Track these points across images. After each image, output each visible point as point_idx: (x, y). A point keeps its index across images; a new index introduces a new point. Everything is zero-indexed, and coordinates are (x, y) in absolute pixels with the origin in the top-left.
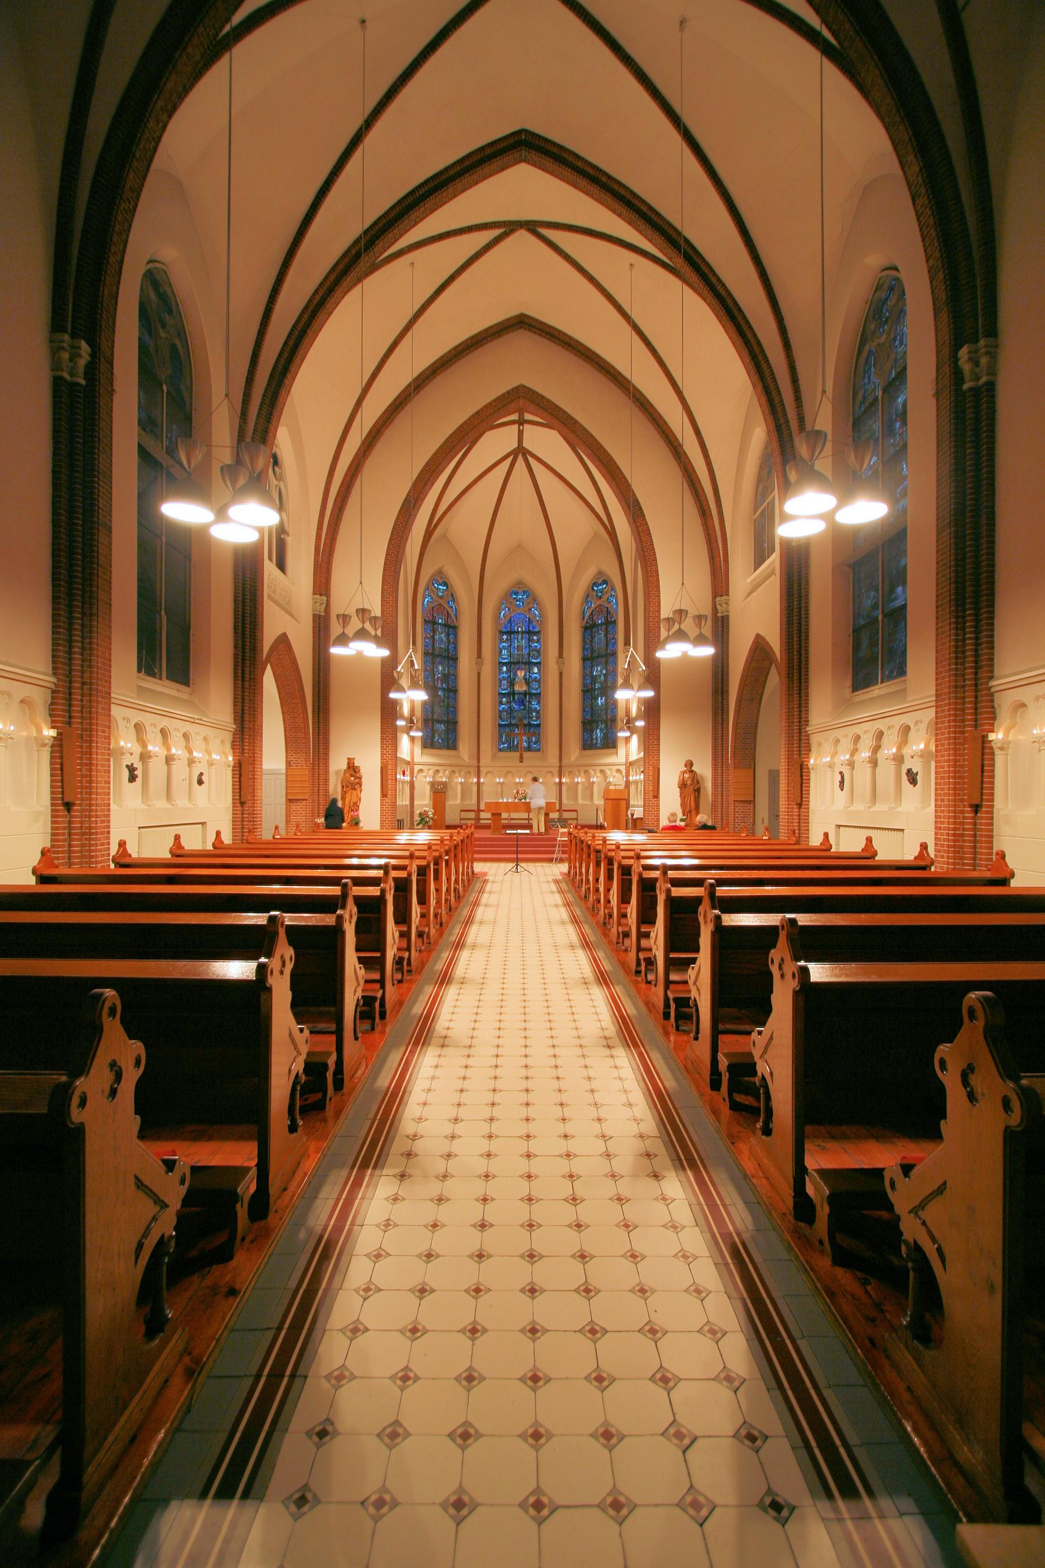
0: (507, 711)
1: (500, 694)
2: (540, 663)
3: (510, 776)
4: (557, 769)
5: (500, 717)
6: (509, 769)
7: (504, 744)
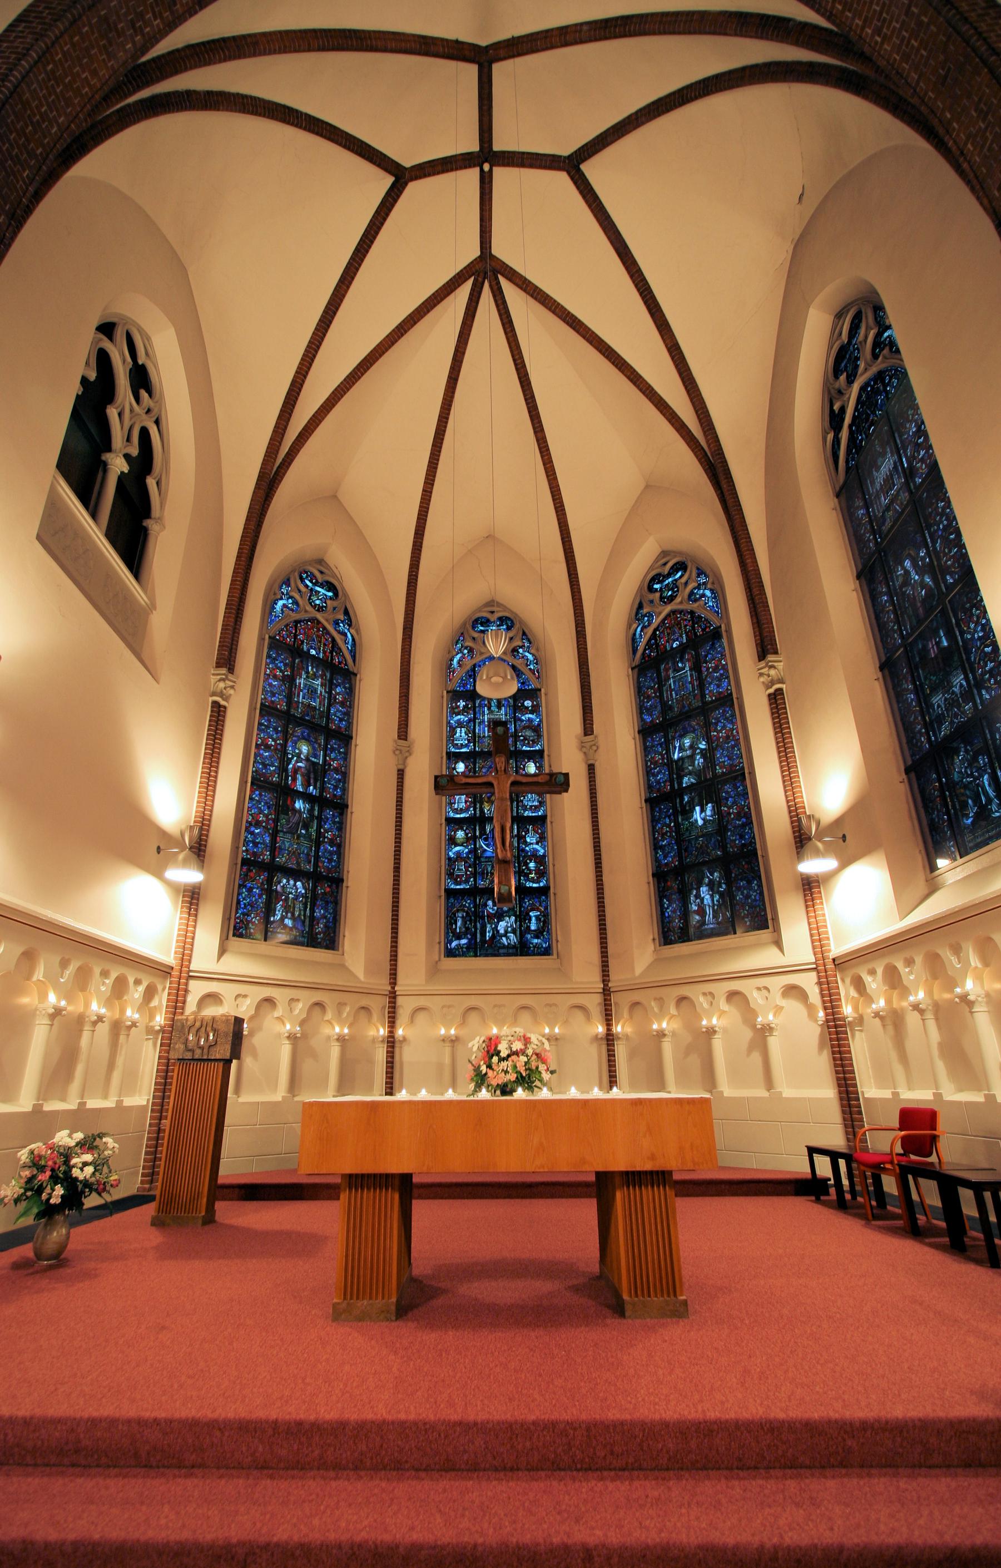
0: (465, 860)
1: (449, 821)
2: (541, 753)
3: (473, 1018)
4: (598, 999)
5: (450, 875)
6: (473, 1001)
7: (459, 937)
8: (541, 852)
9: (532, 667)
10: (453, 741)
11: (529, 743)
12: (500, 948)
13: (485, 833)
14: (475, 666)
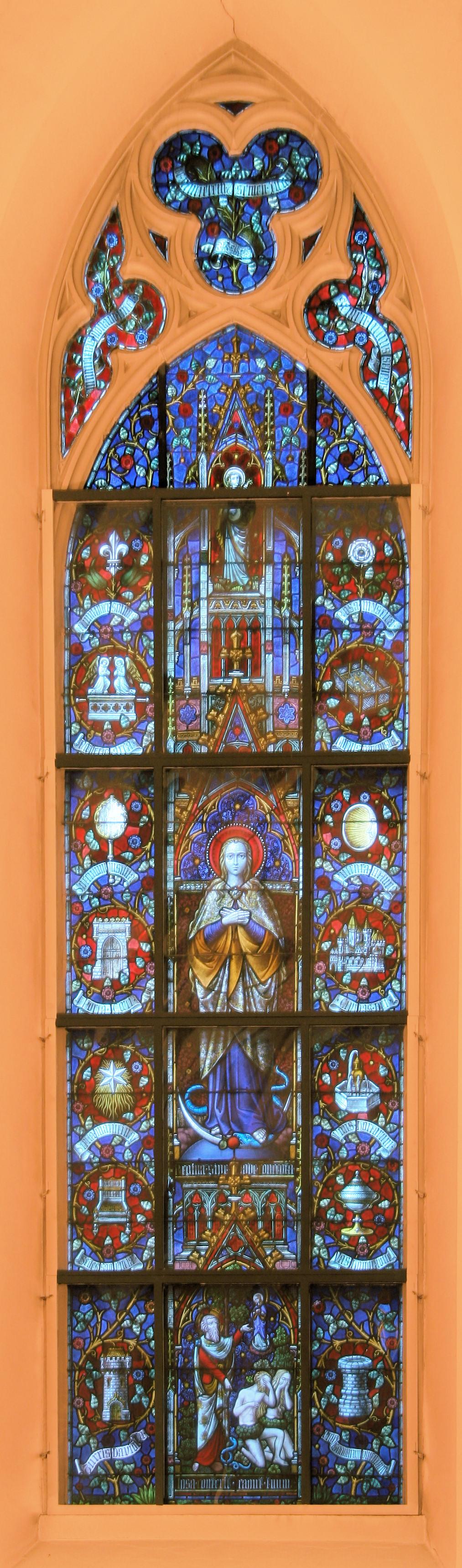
7: (109, 1440)
8: (386, 1148)
9: (383, 383)
10: (83, 708)
11: (357, 724)
12: (239, 1474)
13: (196, 1077)
14: (162, 378)
